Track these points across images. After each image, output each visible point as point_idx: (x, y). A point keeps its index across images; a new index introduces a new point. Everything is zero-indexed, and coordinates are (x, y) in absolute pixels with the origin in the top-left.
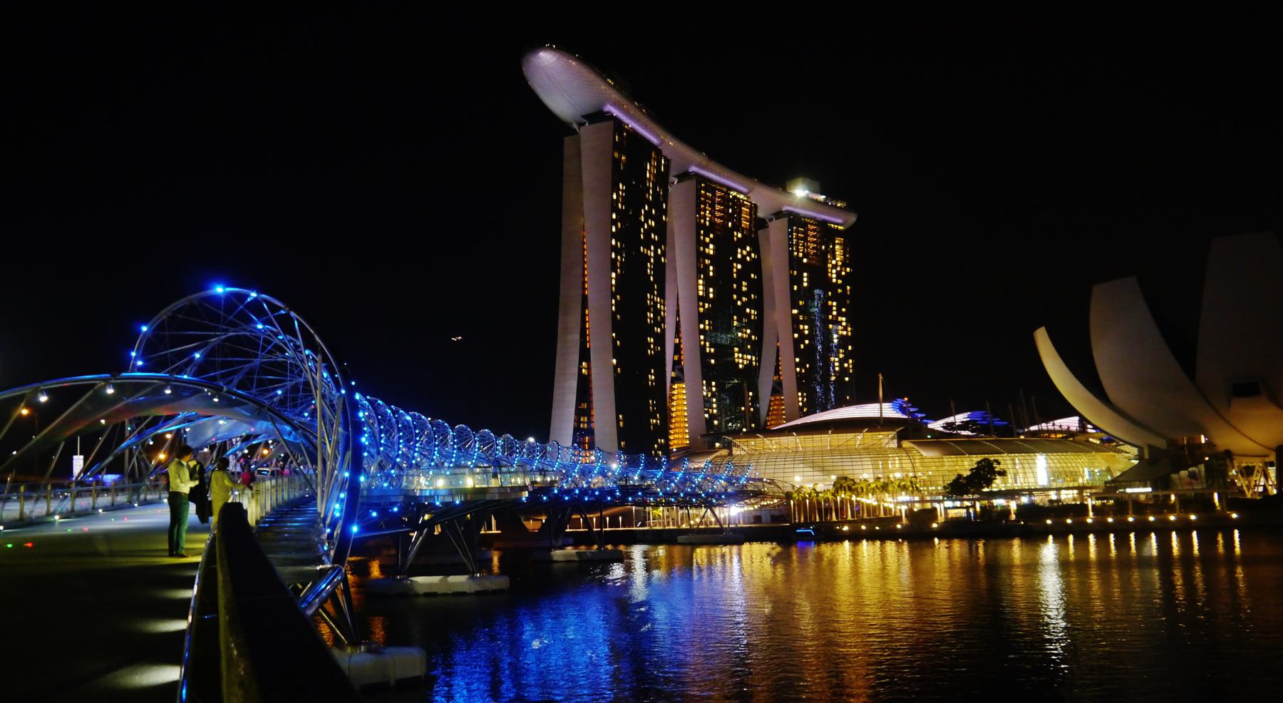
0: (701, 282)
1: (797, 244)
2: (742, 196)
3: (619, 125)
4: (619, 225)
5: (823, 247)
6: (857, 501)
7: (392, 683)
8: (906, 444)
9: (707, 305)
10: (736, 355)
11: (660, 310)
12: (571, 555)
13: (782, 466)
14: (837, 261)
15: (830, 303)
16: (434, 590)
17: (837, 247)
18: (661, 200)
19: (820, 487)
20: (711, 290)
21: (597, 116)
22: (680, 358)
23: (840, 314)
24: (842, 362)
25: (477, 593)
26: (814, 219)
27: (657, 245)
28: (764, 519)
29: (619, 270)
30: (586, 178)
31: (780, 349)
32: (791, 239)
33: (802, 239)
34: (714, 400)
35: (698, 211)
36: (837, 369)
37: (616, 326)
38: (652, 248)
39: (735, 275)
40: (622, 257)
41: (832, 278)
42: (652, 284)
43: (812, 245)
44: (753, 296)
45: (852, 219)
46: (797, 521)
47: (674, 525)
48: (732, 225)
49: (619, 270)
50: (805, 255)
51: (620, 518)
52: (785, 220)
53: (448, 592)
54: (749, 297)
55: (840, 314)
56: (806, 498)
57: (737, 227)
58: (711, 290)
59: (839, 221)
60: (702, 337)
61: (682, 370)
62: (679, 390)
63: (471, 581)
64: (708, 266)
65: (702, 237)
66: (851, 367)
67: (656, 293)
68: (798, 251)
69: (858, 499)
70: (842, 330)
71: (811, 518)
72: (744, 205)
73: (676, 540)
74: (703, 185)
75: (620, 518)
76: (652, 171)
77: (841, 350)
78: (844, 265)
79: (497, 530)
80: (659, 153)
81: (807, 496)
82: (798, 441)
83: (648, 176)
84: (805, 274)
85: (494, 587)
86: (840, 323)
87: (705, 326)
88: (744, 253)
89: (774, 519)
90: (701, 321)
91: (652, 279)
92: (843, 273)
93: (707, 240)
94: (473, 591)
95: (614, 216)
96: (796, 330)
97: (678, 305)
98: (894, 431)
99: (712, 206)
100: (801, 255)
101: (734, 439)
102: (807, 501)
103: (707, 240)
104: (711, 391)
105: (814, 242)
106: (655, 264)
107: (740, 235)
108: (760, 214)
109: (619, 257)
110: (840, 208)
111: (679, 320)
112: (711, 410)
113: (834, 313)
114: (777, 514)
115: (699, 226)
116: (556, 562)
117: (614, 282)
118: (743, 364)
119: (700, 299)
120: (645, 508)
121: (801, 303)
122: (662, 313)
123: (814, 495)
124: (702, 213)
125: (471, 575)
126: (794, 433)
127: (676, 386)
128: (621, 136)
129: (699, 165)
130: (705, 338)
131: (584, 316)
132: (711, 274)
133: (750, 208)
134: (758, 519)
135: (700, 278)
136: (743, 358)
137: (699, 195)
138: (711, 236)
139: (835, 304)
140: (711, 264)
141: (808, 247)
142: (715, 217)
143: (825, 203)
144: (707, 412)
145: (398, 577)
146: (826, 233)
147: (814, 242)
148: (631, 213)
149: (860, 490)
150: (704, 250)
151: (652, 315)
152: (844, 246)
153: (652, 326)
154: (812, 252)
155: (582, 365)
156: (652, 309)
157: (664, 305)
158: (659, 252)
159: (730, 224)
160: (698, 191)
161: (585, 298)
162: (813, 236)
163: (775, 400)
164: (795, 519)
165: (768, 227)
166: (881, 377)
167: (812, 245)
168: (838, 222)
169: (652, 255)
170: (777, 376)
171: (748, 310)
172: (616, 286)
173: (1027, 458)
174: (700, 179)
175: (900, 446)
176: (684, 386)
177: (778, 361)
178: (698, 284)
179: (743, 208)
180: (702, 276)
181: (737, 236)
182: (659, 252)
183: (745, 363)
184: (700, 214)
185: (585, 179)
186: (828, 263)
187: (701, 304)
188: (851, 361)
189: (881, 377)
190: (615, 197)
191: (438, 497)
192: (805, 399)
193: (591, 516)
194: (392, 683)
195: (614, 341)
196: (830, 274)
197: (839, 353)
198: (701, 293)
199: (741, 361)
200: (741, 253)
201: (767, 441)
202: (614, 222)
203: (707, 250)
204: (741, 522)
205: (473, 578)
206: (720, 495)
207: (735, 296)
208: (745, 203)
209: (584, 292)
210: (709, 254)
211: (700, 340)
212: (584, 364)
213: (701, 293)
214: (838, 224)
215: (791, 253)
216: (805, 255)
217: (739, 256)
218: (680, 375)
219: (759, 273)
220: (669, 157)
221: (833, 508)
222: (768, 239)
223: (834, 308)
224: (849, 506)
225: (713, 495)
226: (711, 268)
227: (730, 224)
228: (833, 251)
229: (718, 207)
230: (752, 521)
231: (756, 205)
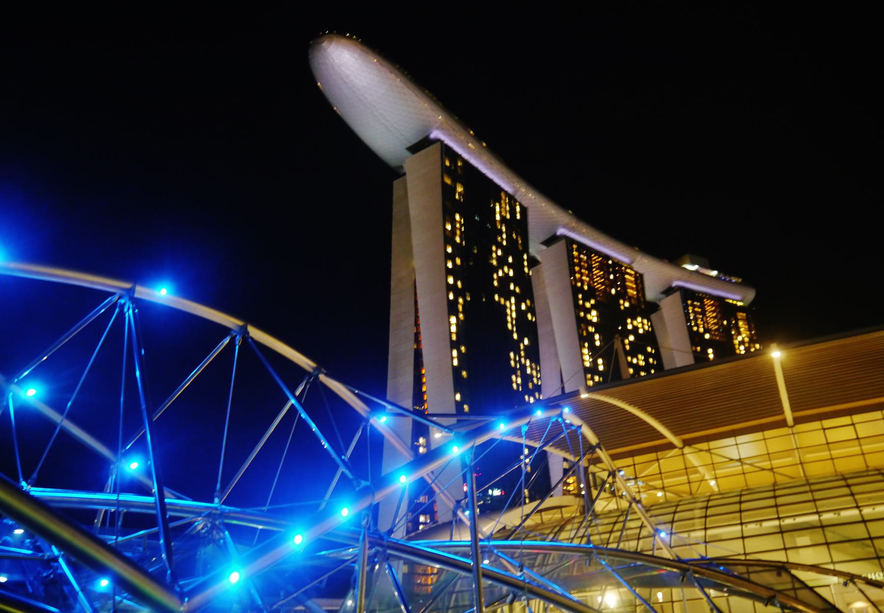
0: (585, 351)
1: (696, 319)
3: (448, 152)
5: (725, 322)
11: (531, 376)
17: (741, 323)
18: (520, 248)
20: (600, 361)
30: (413, 212)
32: (687, 315)
35: (572, 273)
43: (712, 321)
45: (751, 295)
50: (707, 330)
57: (623, 294)
58: (600, 361)
64: (592, 334)
65: (581, 302)
67: (522, 353)
68: (697, 325)
95: (449, 250)
97: (562, 381)
100: (701, 330)
103: (588, 305)
110: (736, 283)
115: (576, 291)
117: (454, 329)
119: (587, 370)
129: (565, 226)
132: (598, 343)
137: (571, 257)
140: (596, 332)
146: (726, 310)
148: (476, 251)
150: (585, 316)
151: (519, 381)
152: (748, 321)
159: (613, 291)
167: (712, 321)
168: (737, 298)
172: (457, 333)
174: (570, 241)
178: (582, 354)
180: (586, 345)
182: (523, 307)
184: (575, 277)
187: (589, 376)
190: (449, 227)
198: (587, 364)
202: (448, 257)
208: (628, 271)
215: (690, 328)
216: (707, 330)
219: (655, 346)
220: (525, 204)
222: (661, 319)
226: (597, 337)
228: (736, 325)
231: (641, 276)
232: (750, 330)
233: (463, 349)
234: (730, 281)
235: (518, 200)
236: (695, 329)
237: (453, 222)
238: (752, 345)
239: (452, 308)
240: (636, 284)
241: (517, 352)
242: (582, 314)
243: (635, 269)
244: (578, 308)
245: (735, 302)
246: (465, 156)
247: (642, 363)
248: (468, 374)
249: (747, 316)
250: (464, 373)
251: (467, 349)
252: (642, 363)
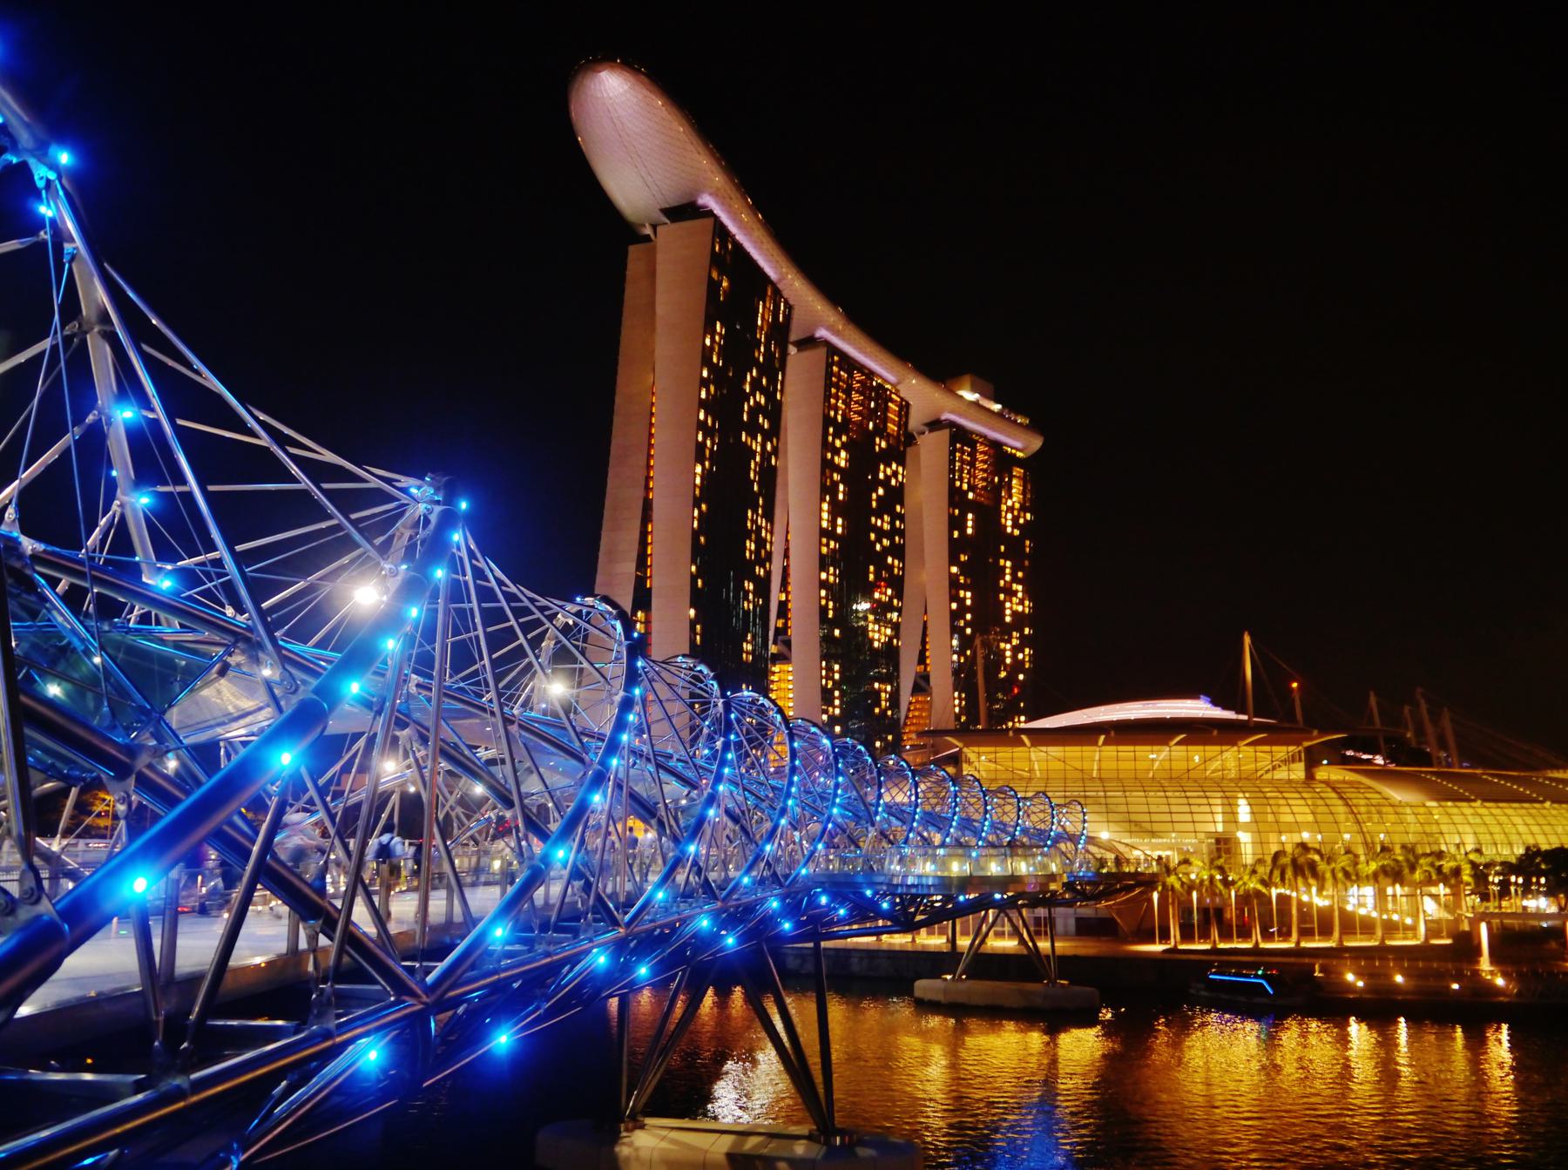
0: (825, 506)
1: (961, 470)
2: (888, 386)
3: (721, 232)
4: (712, 388)
5: (996, 479)
8: (1325, 772)
9: (832, 544)
10: (871, 627)
11: (765, 540)
14: (1014, 503)
15: (1002, 562)
17: (1015, 482)
18: (777, 365)
20: (840, 521)
21: (685, 211)
22: (785, 624)
23: (1015, 579)
24: (1016, 650)
26: (985, 437)
27: (767, 436)
29: (707, 463)
31: (929, 624)
32: (952, 462)
34: (837, 693)
36: (1008, 661)
37: (697, 552)
38: (759, 439)
39: (874, 504)
40: (713, 443)
41: (1006, 527)
42: (756, 496)
43: (981, 475)
44: (897, 538)
45: (1036, 443)
48: (874, 428)
49: (707, 463)
50: (972, 488)
52: (944, 435)
54: (892, 541)
55: (1015, 579)
57: (881, 431)
58: (840, 521)
59: (1018, 445)
60: (823, 593)
61: (788, 644)
62: (782, 675)
65: (830, 438)
66: (1027, 659)
67: (760, 512)
68: (961, 479)
70: (1017, 604)
72: (892, 401)
74: (836, 358)
76: (766, 317)
77: (1014, 634)
78: (1023, 509)
80: (777, 293)
83: (759, 323)
84: (970, 516)
86: (1015, 593)
87: (829, 576)
88: (889, 471)
90: (823, 567)
91: (756, 488)
92: (1021, 521)
93: (838, 443)
95: (705, 374)
96: (954, 597)
98: (1298, 744)
99: (848, 392)
100: (965, 487)
101: (967, 745)
104: (833, 679)
105: (984, 471)
106: (761, 465)
107: (883, 444)
109: (709, 443)
110: (1021, 425)
111: (788, 565)
112: (831, 709)
113: (1008, 578)
115: (828, 421)
117: (698, 481)
118: (879, 640)
121: (963, 558)
122: (768, 547)
124: (833, 401)
128: (723, 246)
129: (831, 328)
130: (827, 594)
131: (644, 534)
132: (841, 497)
133: (900, 406)
135: (825, 500)
136: (879, 631)
137: (829, 374)
138: (844, 438)
139: (1008, 564)
141: (975, 477)
142: (850, 410)
143: (1000, 415)
144: (825, 712)
146: (1002, 461)
147: (984, 471)
151: (753, 547)
152: (1024, 480)
153: (752, 564)
154: (981, 484)
155: (636, 616)
156: (753, 536)
157: (772, 533)
158: (769, 447)
159: (871, 425)
160: (829, 366)
161: (647, 506)
162: (984, 462)
163: (917, 702)
165: (916, 444)
166: (1247, 640)
167: (981, 475)
168: (1020, 444)
169: (759, 449)
170: (923, 667)
171: (890, 560)
172: (702, 487)
173: (1494, 811)
174: (832, 350)
175: (1310, 776)
176: (790, 669)
177: (924, 643)
178: (821, 510)
179: (890, 404)
180: (828, 498)
181: (880, 445)
182: (769, 447)
183: (882, 641)
185: (661, 309)
186: (1000, 503)
187: (824, 540)
188: (1027, 651)
189: (1247, 640)
190: (708, 342)
192: (964, 703)
195: (694, 578)
196: (1003, 520)
197: (1011, 637)
198: (825, 524)
199: (876, 636)
200: (885, 472)
202: (704, 383)
203: (836, 458)
207: (873, 536)
208: (894, 396)
209: (648, 494)
210: (838, 466)
211: (820, 598)
212: (640, 614)
213: (825, 524)
214: (1017, 449)
215: (952, 481)
217: (881, 476)
218: (784, 649)
220: (791, 302)
223: (1008, 571)
227: (871, 425)
228: (1010, 488)
229: (855, 396)
231: (908, 405)
232: (1024, 493)
233: (704, 507)
234: (1015, 421)
235: (786, 294)
236: (958, 484)
237: (713, 333)
238: (1022, 514)
239: (700, 458)
240: (900, 416)
241: (755, 511)
242: (829, 455)
243: (902, 395)
244: (827, 446)
245: (1014, 451)
246: (740, 237)
247: (886, 527)
248: (706, 540)
249: (1025, 473)
250: (702, 539)
251: (708, 509)
252: (886, 527)
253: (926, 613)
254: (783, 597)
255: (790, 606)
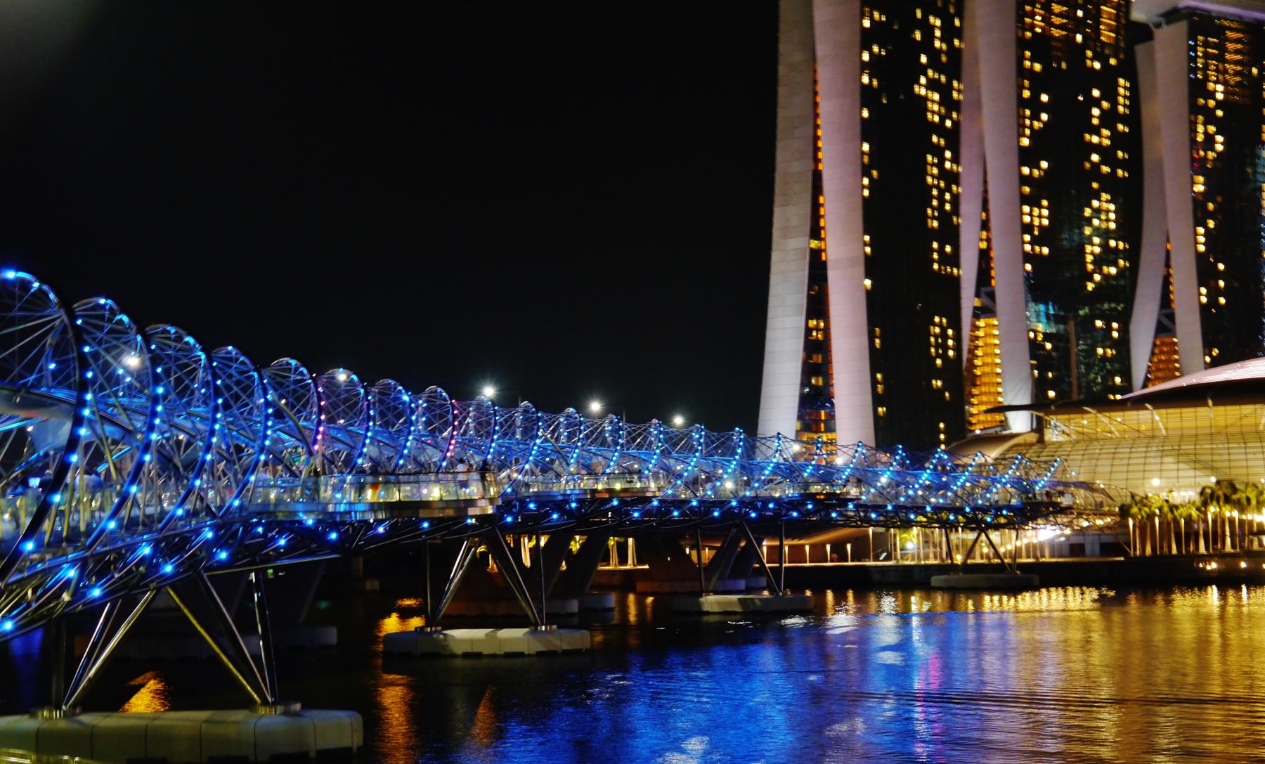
1: (1206, 67)
6: (1242, 522)
7: (313, 754)
12: (730, 603)
13: (1125, 462)
16: (476, 650)
19: (1178, 497)
25: (539, 654)
26: (1240, 19)
28: (1088, 549)
32: (1194, 60)
33: (1213, 57)
46: (1138, 553)
47: (935, 558)
51: (849, 547)
52: (1181, 27)
53: (498, 653)
56: (1154, 514)
57: (1093, 38)
61: (992, 296)
62: (987, 329)
63: (530, 637)
69: (1244, 517)
71: (1161, 548)
73: (929, 584)
75: (849, 547)
79: (640, 561)
81: (1157, 511)
82: (1157, 418)
85: (565, 647)
89: (1107, 548)
94: (533, 651)
97: (985, 182)
102: (1157, 520)
105: (1236, 63)
108: (1137, 15)
114: (1108, 539)
115: (1022, 44)
116: (708, 613)
120: (888, 530)
123: (1166, 509)
125: (533, 628)
126: (1148, 405)
127: (981, 323)
131: (816, 206)
134: (1076, 549)
135: (1024, 135)
145: (429, 630)
147: (1236, 63)
149: (1244, 501)
154: (1233, 80)
159: (1079, 38)
161: (817, 177)
162: (1237, 52)
163: (1163, 344)
164: (1135, 549)
176: (996, 323)
191: (356, 512)
193: (802, 542)
194: (313, 754)
201: (1103, 418)
204: (1047, 553)
205: (535, 632)
206: (999, 509)
211: (1024, 242)
218: (988, 302)
221: (1201, 532)
224: (1227, 529)
225: (985, 510)
227: (1079, 38)
230: (1066, 550)
233: (875, 173)
253: (1168, 241)
254: (983, 245)
255: (993, 254)
